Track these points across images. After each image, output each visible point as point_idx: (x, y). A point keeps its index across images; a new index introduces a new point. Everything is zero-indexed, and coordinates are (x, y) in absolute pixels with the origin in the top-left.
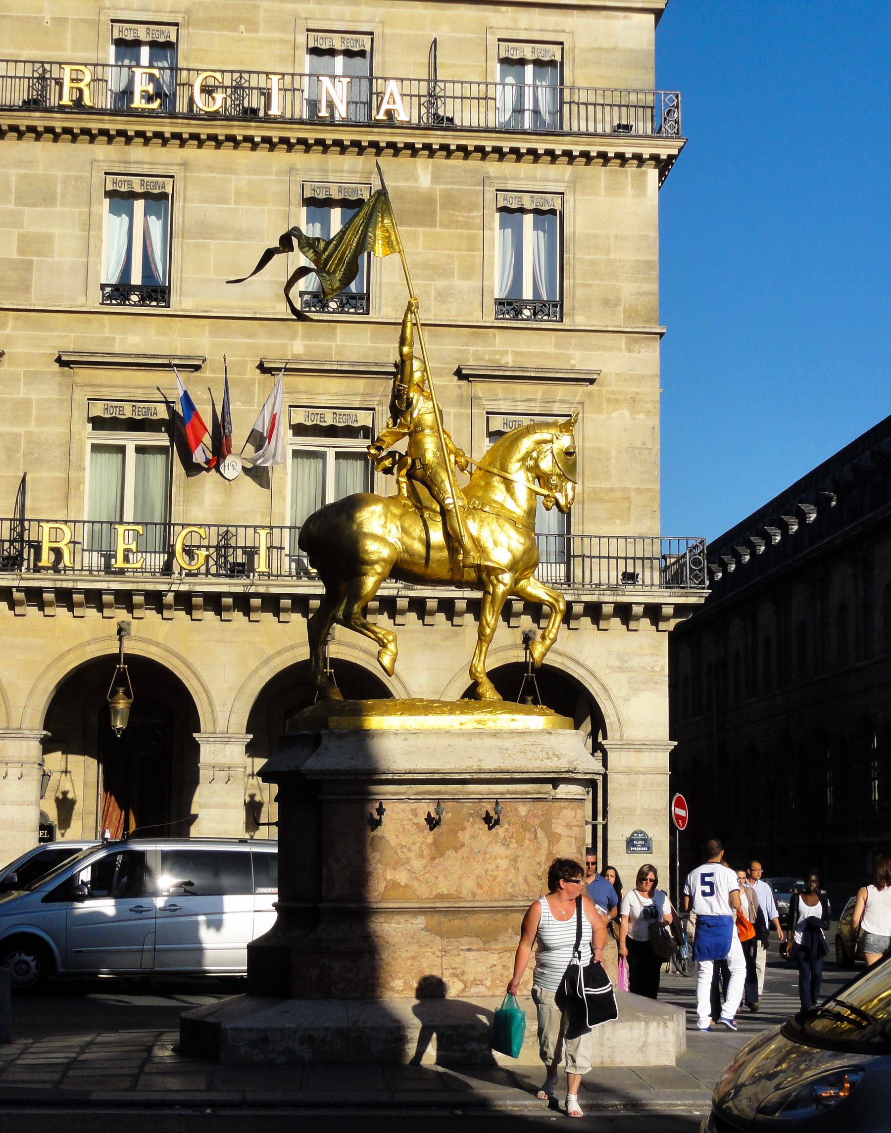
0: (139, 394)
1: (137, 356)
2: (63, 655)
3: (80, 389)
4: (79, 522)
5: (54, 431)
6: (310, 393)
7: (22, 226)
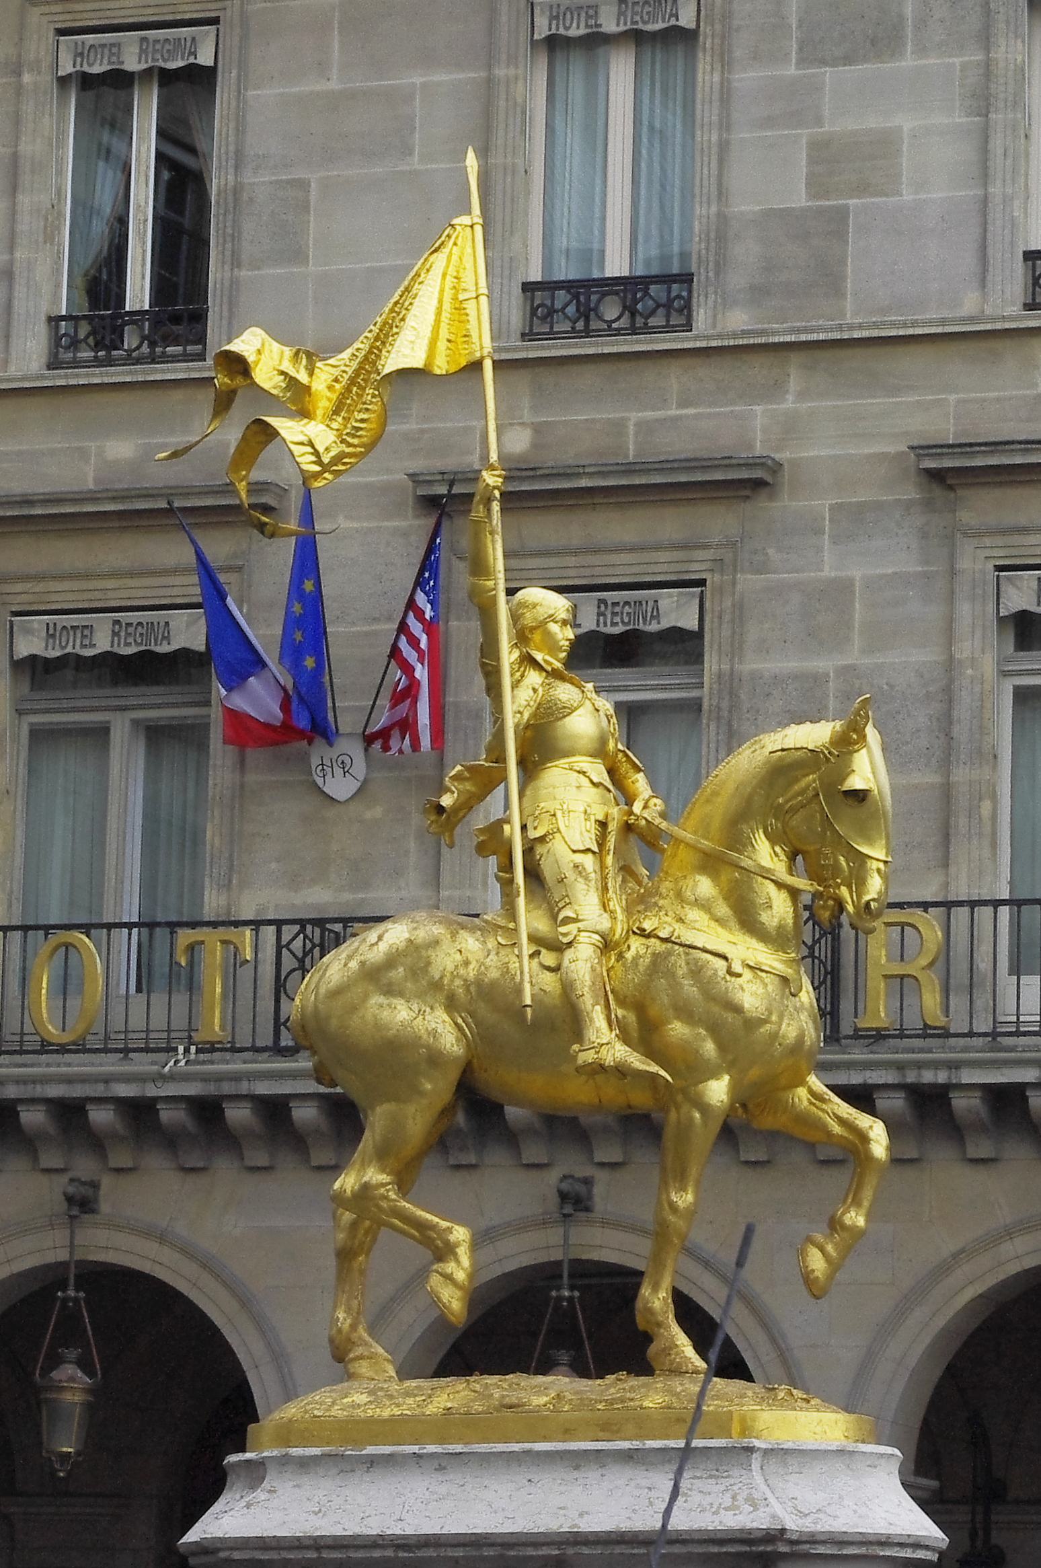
4: (984, 903)
5: (910, 660)
7: (819, 121)
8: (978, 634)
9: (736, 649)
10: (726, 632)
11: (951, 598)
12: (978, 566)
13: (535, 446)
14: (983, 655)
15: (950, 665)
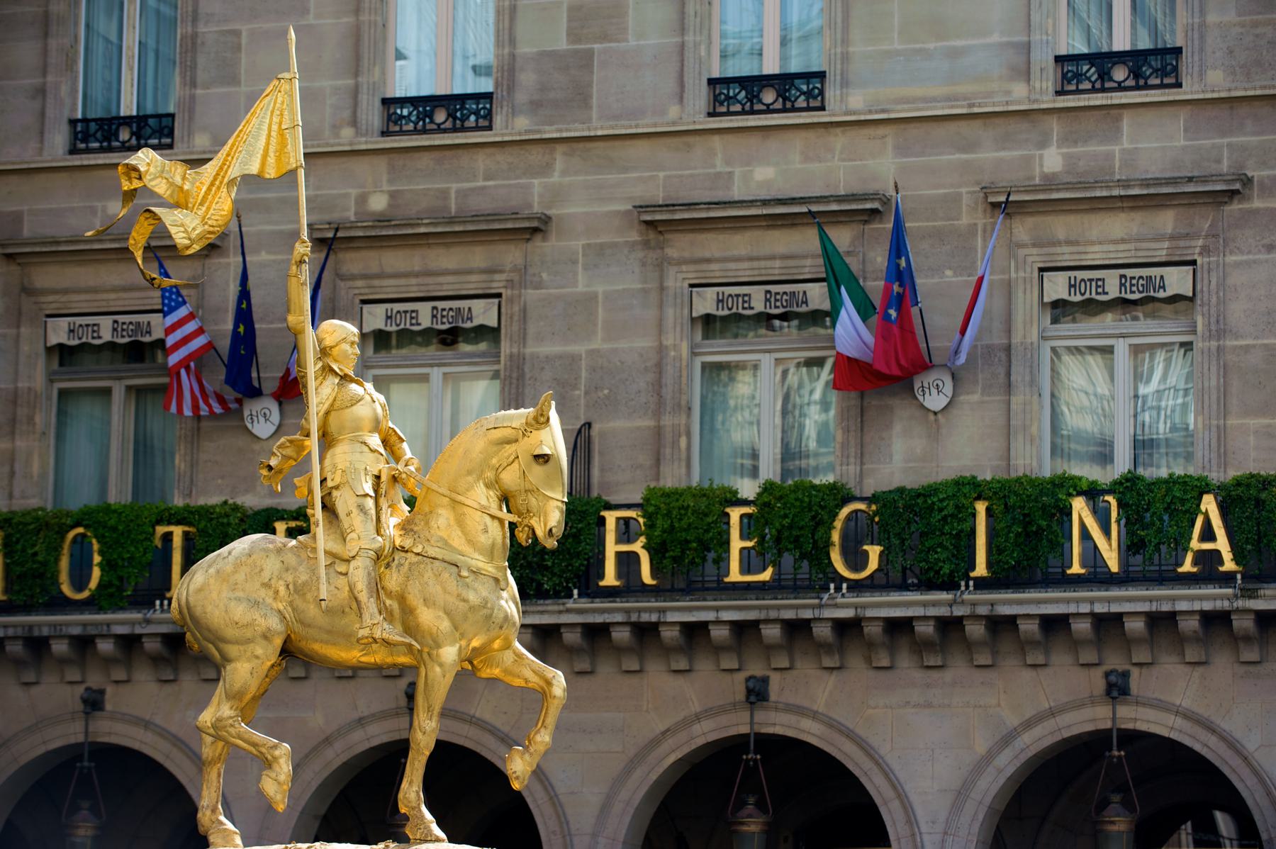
0: (775, 269)
1: (765, 203)
2: (655, 742)
3: (676, 268)
6: (1077, 243)
8: (678, 329)
9: (523, 338)
10: (515, 327)
11: (661, 306)
12: (679, 284)
13: (390, 205)
14: (679, 342)
15: (661, 349)
